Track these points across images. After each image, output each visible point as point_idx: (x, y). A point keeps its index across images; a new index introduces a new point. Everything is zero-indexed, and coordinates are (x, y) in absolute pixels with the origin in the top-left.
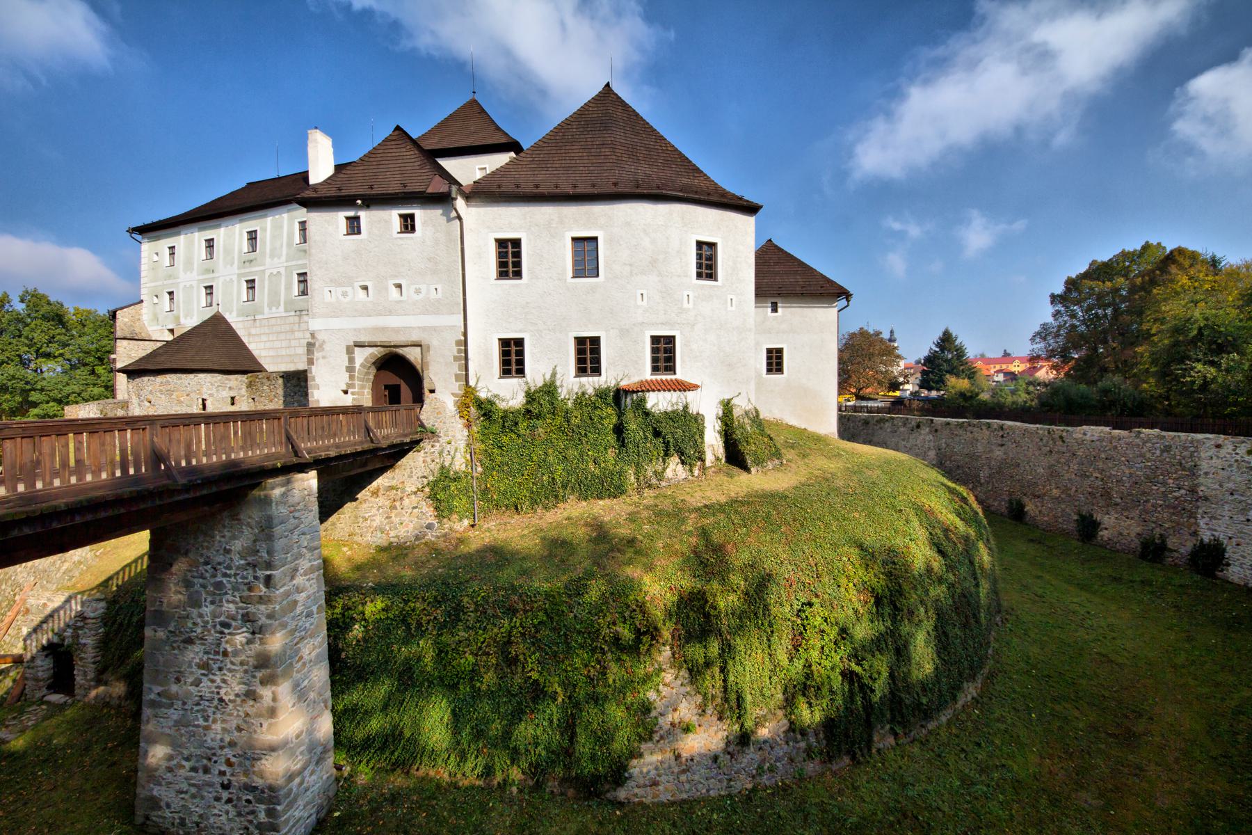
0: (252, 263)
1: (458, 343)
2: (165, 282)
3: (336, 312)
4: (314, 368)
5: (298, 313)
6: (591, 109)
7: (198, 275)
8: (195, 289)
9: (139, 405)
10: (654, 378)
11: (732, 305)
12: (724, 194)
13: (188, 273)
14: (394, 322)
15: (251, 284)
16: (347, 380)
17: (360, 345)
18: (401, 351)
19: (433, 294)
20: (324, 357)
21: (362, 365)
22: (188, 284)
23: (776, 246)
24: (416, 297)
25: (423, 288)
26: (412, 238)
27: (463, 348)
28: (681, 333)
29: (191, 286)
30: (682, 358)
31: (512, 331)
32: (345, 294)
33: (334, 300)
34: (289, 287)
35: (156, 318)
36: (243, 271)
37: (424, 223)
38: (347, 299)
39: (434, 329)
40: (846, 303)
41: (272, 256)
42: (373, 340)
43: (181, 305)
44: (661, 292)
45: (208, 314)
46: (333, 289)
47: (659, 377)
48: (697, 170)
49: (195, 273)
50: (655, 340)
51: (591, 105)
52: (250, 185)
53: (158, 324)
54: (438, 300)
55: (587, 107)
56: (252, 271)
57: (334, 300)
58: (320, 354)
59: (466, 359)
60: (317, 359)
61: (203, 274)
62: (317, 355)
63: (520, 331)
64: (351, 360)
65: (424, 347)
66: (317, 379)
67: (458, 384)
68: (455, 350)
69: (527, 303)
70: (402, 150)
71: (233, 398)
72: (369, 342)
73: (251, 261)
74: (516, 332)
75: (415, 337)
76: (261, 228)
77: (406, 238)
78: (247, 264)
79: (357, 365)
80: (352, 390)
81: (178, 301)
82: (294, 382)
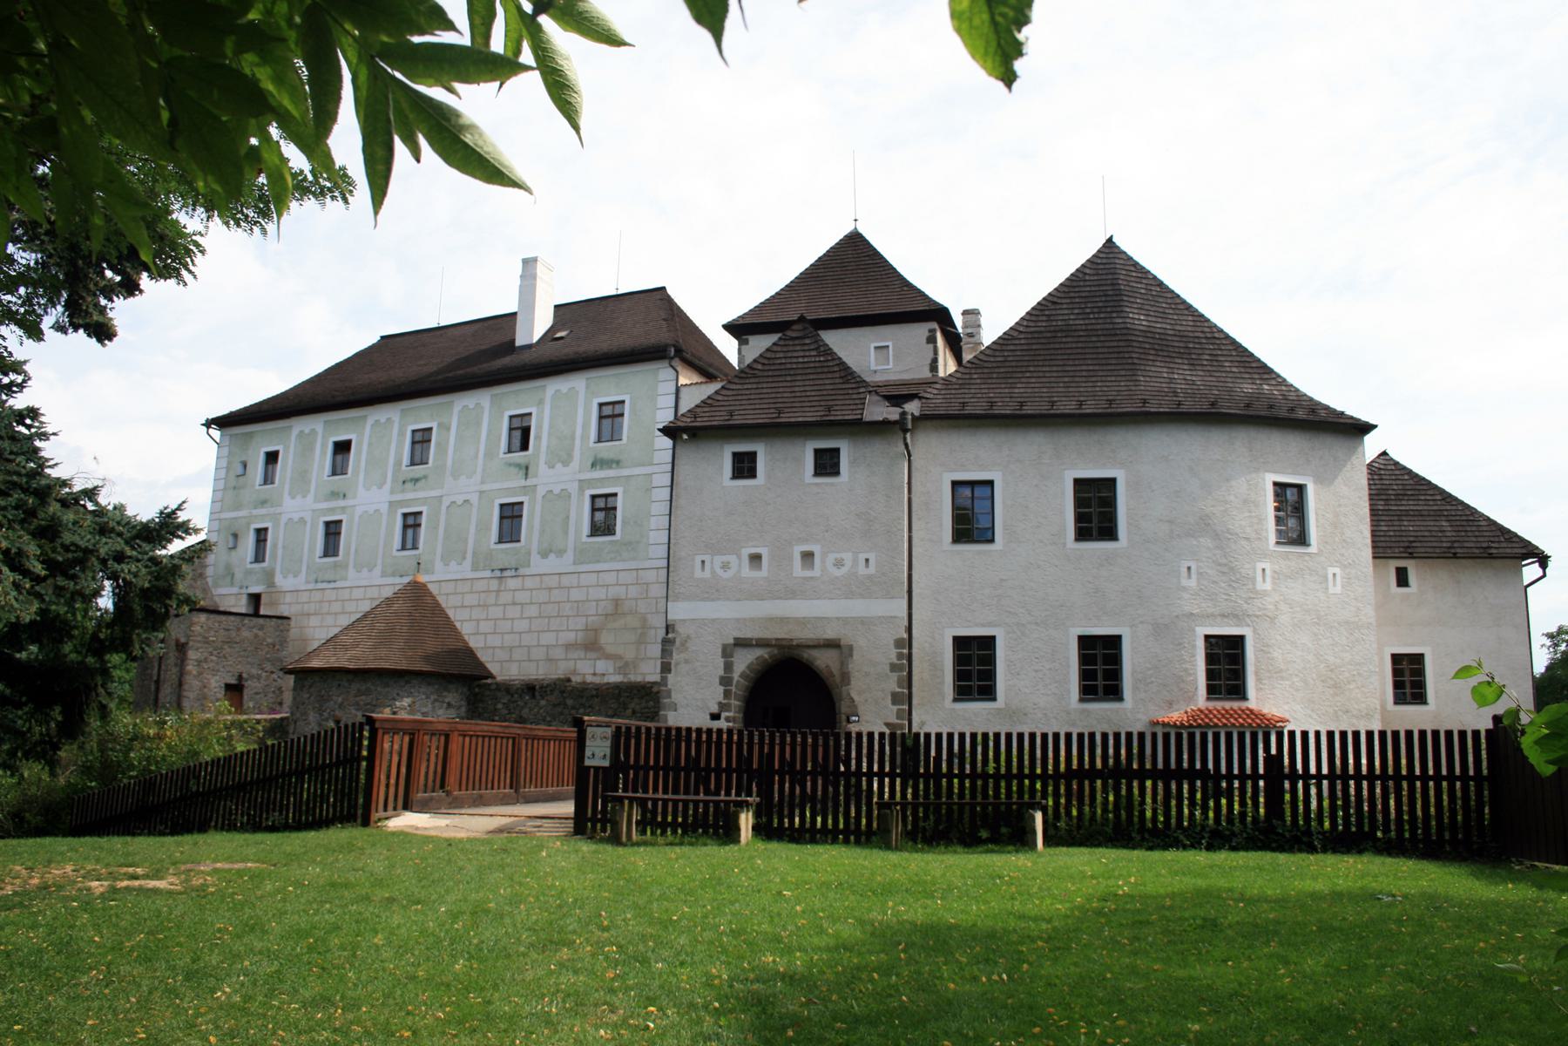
0: (419, 484)
2: (255, 512)
3: (711, 592)
4: (671, 677)
5: (498, 574)
6: (1087, 278)
7: (316, 500)
8: (309, 525)
10: (1211, 705)
11: (1334, 585)
12: (1314, 406)
13: (299, 497)
15: (411, 522)
16: (721, 698)
17: (741, 643)
18: (806, 655)
19: (862, 570)
20: (686, 661)
21: (742, 675)
22: (296, 517)
23: (1396, 463)
25: (847, 557)
26: (832, 484)
28: (1255, 631)
29: (302, 521)
30: (1256, 673)
31: (977, 625)
32: (725, 566)
34: (483, 527)
37: (853, 463)
39: (863, 621)
40: (1540, 572)
41: (455, 476)
42: (765, 636)
44: (1220, 565)
46: (707, 558)
47: (1219, 705)
48: (1264, 371)
49: (311, 497)
51: (1088, 271)
52: (383, 338)
53: (232, 584)
54: (870, 577)
55: (1081, 275)
56: (415, 499)
57: (707, 574)
58: (682, 655)
60: (677, 664)
62: (676, 657)
63: (990, 624)
64: (728, 667)
67: (895, 708)
69: (1002, 580)
72: (757, 640)
73: (416, 480)
74: (983, 625)
75: (830, 633)
76: (440, 425)
77: (827, 484)
78: (409, 485)
79: (736, 676)
80: (727, 714)
81: (275, 546)
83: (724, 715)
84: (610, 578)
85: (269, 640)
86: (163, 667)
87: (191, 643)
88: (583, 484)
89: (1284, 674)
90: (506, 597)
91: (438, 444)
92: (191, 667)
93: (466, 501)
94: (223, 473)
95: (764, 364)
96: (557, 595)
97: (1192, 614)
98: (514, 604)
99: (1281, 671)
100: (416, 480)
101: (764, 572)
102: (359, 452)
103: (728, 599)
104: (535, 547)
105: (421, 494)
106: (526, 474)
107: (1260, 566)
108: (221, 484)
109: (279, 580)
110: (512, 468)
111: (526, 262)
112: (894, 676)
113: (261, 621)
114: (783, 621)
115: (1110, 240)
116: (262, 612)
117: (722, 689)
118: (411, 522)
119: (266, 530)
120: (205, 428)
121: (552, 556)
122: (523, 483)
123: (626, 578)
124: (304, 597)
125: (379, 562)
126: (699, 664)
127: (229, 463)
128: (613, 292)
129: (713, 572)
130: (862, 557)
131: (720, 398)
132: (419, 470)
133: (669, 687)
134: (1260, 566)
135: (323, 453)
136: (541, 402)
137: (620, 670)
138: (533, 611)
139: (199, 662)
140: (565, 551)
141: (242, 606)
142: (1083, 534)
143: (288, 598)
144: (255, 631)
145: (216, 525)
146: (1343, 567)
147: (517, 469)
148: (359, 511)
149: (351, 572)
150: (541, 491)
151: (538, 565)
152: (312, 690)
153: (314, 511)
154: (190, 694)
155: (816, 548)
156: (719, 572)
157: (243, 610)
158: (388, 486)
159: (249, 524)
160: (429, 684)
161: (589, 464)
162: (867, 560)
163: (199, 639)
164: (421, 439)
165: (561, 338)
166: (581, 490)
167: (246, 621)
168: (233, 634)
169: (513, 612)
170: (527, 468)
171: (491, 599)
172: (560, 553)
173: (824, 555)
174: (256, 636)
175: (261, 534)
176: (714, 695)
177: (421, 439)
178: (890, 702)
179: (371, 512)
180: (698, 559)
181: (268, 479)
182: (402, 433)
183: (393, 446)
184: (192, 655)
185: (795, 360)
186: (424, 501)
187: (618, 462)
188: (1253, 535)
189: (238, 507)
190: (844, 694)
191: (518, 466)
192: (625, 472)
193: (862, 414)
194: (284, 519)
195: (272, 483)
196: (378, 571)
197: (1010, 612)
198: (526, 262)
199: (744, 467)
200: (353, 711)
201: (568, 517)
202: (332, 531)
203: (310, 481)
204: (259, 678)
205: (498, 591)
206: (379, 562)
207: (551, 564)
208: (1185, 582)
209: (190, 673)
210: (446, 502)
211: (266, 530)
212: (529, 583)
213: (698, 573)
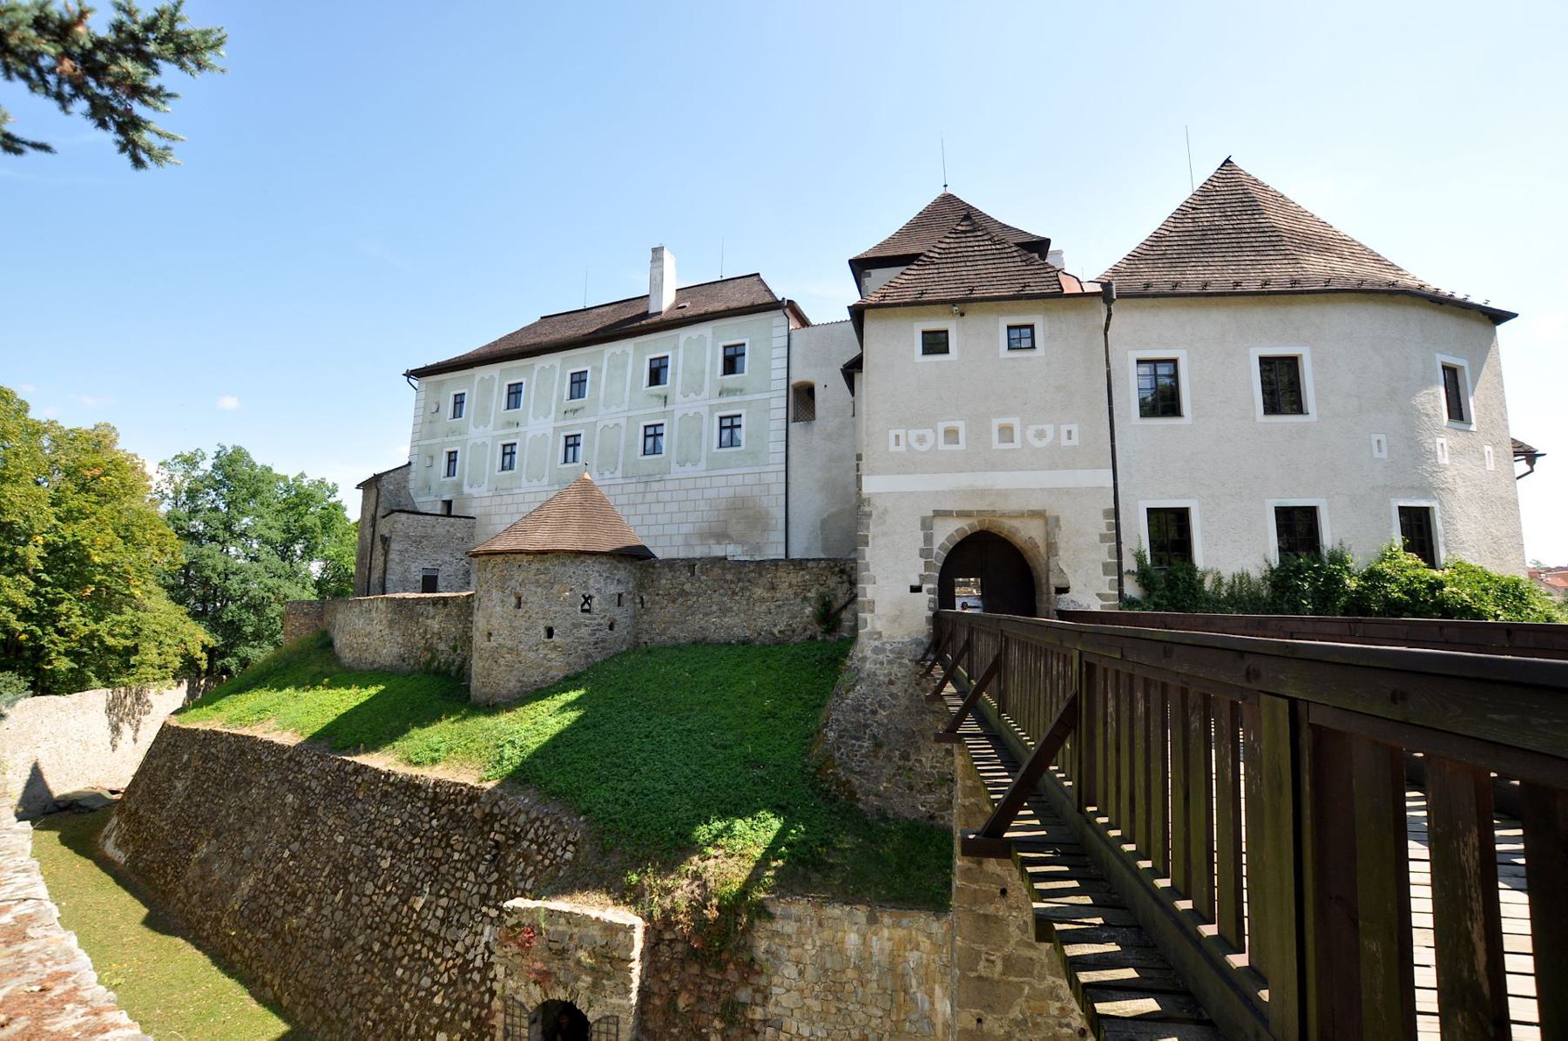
0: (579, 413)
1: (1106, 514)
3: (907, 464)
9: (502, 601)
13: (481, 428)
14: (1002, 480)
15: (572, 443)
17: (938, 514)
19: (1065, 442)
20: (884, 534)
21: (939, 548)
24: (1038, 444)
25: (1049, 429)
26: (1028, 359)
28: (1441, 503)
32: (922, 440)
33: (902, 448)
36: (562, 424)
37: (1049, 337)
39: (1068, 492)
40: (1528, 468)
46: (901, 432)
56: (574, 425)
59: (1119, 543)
60: (874, 537)
63: (1183, 497)
64: (928, 539)
66: (871, 568)
68: (1102, 525)
71: (620, 595)
74: (1176, 498)
75: (1035, 506)
81: (463, 463)
82: (717, 571)
83: (925, 587)
84: (738, 480)
85: (459, 535)
86: (374, 557)
87: (393, 537)
88: (712, 409)
89: (1466, 545)
90: (650, 497)
91: (592, 383)
92: (393, 556)
93: (617, 425)
95: (939, 254)
96: (693, 495)
97: (1386, 486)
98: (658, 502)
99: (1463, 543)
100: (576, 410)
101: (962, 446)
102: (529, 392)
105: (579, 421)
107: (1439, 441)
109: (466, 490)
111: (655, 250)
113: (452, 520)
114: (982, 493)
115: (1228, 161)
117: (922, 561)
118: (572, 443)
119: (456, 452)
121: (688, 465)
123: (749, 480)
124: (486, 502)
125: (547, 473)
127: (426, 404)
128: (720, 279)
129: (908, 445)
130: (1064, 429)
132: (577, 402)
133: (867, 559)
134: (1439, 441)
135: (500, 393)
136: (676, 347)
137: (745, 553)
138: (674, 507)
139: (401, 551)
140: (700, 460)
141: (439, 509)
142: (1271, 407)
143: (476, 503)
144: (447, 528)
145: (416, 450)
146: (1494, 445)
147: (657, 400)
148: (529, 435)
150: (678, 414)
152: (495, 570)
153: (493, 437)
154: (393, 577)
155: (1015, 422)
156: (916, 446)
157: (439, 512)
158: (552, 416)
159: (442, 448)
162: (1069, 432)
163: (402, 533)
164: (578, 381)
166: (711, 413)
167: (440, 519)
168: (429, 530)
169: (657, 508)
170: (666, 397)
171: (639, 498)
174: (448, 531)
175: (452, 457)
177: (578, 381)
178: (1102, 573)
179: (540, 435)
180: (892, 434)
181: (457, 413)
184: (394, 546)
186: (582, 426)
187: (741, 390)
188: (1431, 412)
189: (432, 436)
190: (1052, 564)
191: (659, 396)
192: (748, 398)
193: (1062, 288)
194: (469, 444)
195: (460, 416)
196: (545, 481)
198: (655, 250)
199: (935, 343)
200: (534, 589)
201: (701, 434)
202: (508, 451)
203: (490, 415)
206: (547, 473)
208: (1376, 455)
209: (393, 560)
211: (456, 452)
212: (670, 485)
213: (892, 448)
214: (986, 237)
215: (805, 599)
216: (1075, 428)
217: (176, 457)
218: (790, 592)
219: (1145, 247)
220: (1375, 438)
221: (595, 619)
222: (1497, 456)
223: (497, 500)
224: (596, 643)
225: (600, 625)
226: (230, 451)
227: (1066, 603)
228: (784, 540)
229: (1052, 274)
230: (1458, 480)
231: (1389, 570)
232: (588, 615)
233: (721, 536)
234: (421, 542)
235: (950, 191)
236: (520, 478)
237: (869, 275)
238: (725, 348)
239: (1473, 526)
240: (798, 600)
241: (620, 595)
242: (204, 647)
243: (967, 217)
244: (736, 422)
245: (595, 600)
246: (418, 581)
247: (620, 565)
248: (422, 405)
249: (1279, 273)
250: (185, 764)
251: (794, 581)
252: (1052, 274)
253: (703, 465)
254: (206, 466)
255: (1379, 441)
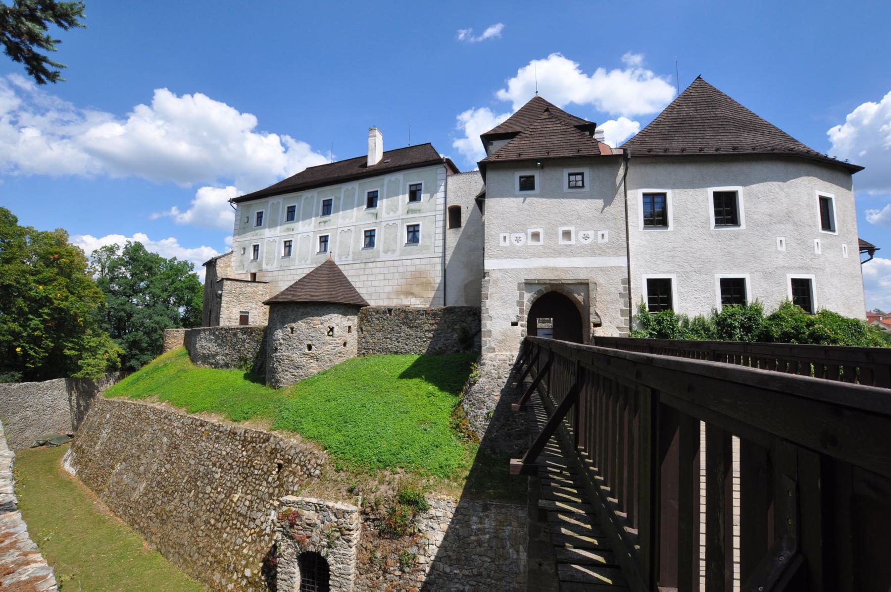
0: (327, 223)
2: (253, 238)
3: (511, 253)
8: (277, 242)
15: (324, 240)
17: (529, 284)
19: (600, 240)
21: (528, 301)
25: (591, 233)
26: (581, 193)
27: (627, 286)
30: (818, 300)
31: (660, 272)
32: (518, 240)
34: (357, 241)
35: (242, 265)
38: (521, 243)
39: (602, 269)
40: (869, 257)
43: (264, 255)
44: (797, 239)
45: (323, 258)
46: (507, 235)
50: (795, 282)
52: (309, 169)
54: (605, 244)
59: (630, 299)
61: (284, 231)
64: (521, 296)
65: (591, 286)
67: (624, 318)
68: (621, 288)
70: (558, 125)
71: (350, 327)
73: (326, 222)
74: (664, 273)
75: (582, 276)
78: (322, 224)
79: (525, 301)
81: (262, 252)
83: (520, 323)
90: (368, 271)
91: (335, 206)
94: (238, 222)
96: (392, 270)
100: (326, 222)
101: (541, 242)
103: (520, 258)
104: (381, 249)
106: (376, 217)
107: (816, 241)
108: (238, 227)
109: (264, 267)
110: (370, 215)
112: (622, 300)
113: (256, 284)
114: (554, 269)
115: (699, 77)
116: (257, 280)
118: (324, 240)
119: (258, 245)
120: (229, 203)
122: (375, 221)
124: (276, 273)
126: (505, 294)
128: (408, 146)
130: (600, 233)
131: (507, 148)
135: (283, 212)
136: (382, 185)
139: (227, 302)
140: (395, 250)
146: (848, 244)
149: (297, 263)
151: (383, 257)
155: (572, 229)
157: (250, 280)
160: (339, 309)
161: (406, 211)
162: (603, 235)
163: (227, 292)
165: (388, 162)
166: (403, 223)
168: (243, 290)
170: (377, 215)
171: (362, 272)
172: (394, 251)
173: (577, 233)
174: (254, 291)
175: (256, 248)
176: (513, 312)
180: (502, 236)
182: (318, 202)
183: (314, 208)
184: (224, 298)
185: (548, 129)
187: (419, 210)
196: (309, 262)
197: (679, 265)
204: (256, 308)
205: (365, 269)
207: (390, 256)
208: (779, 248)
210: (339, 230)
211: (258, 245)
213: (502, 243)
214: (557, 122)
215: (454, 330)
216: (606, 233)
217: (103, 247)
218: (445, 325)
219: (649, 128)
220: (779, 239)
221: (335, 340)
222: (850, 250)
223: (282, 273)
224: (336, 354)
225: (338, 343)
226: (133, 244)
227: (599, 332)
228: (443, 296)
229: (594, 144)
230: (827, 264)
231: (784, 315)
232: (331, 338)
233: (409, 294)
234: (238, 296)
235: (539, 95)
236: (295, 259)
237: (492, 144)
238: (410, 186)
239: (834, 290)
240: (450, 330)
241: (350, 327)
242: (119, 355)
243: (547, 110)
244: (416, 229)
245: (335, 330)
246: (237, 319)
247: (349, 310)
248: (239, 218)
249: (725, 142)
250: (108, 420)
251: (447, 320)
252: (594, 144)
253: (398, 253)
254: (120, 253)
255: (781, 241)
